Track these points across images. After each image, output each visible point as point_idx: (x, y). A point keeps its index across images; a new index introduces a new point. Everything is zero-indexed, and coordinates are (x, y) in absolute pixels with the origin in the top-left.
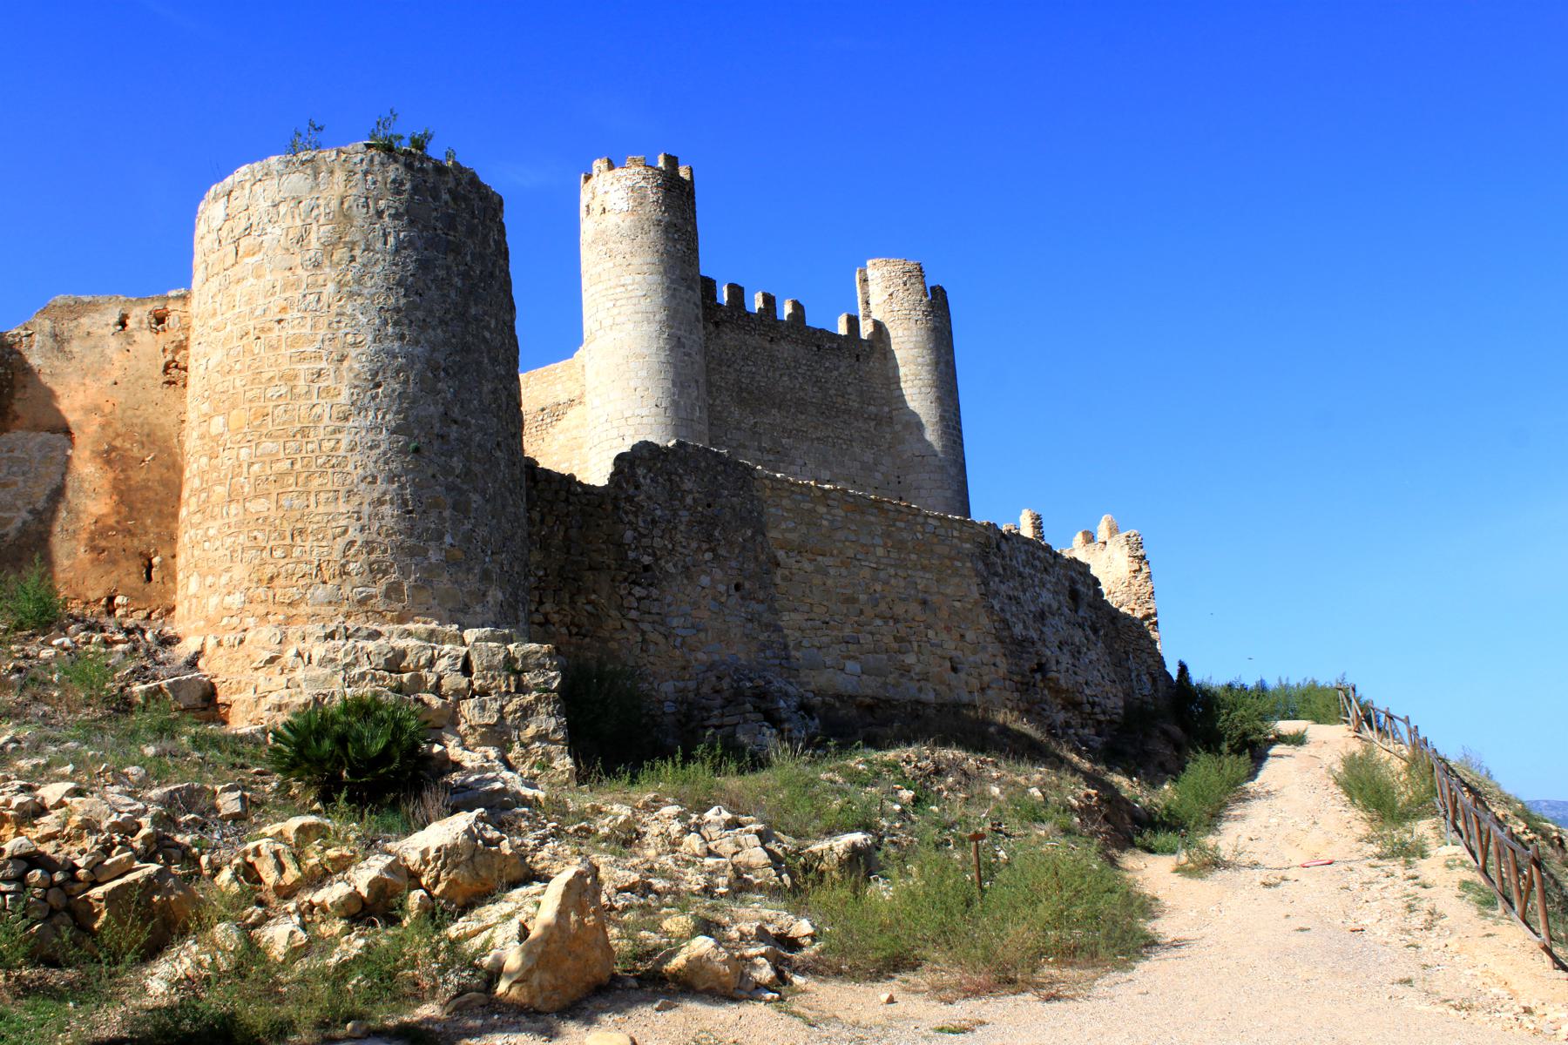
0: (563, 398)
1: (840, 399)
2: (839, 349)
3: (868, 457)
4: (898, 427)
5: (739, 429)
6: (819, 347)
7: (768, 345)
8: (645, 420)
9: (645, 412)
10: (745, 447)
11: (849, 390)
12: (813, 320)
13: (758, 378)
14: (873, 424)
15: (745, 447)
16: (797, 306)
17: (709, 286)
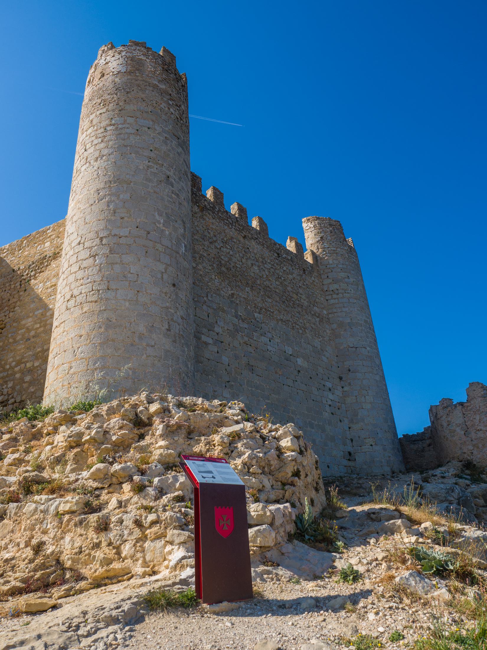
0: (49, 253)
1: (295, 296)
2: (292, 260)
3: (317, 343)
4: (335, 326)
5: (219, 295)
6: (278, 254)
7: (242, 239)
8: (123, 241)
9: (124, 232)
10: (223, 311)
11: (301, 291)
12: (273, 235)
13: (234, 260)
14: (318, 319)
15: (223, 311)
16: (261, 222)
17: (196, 183)
